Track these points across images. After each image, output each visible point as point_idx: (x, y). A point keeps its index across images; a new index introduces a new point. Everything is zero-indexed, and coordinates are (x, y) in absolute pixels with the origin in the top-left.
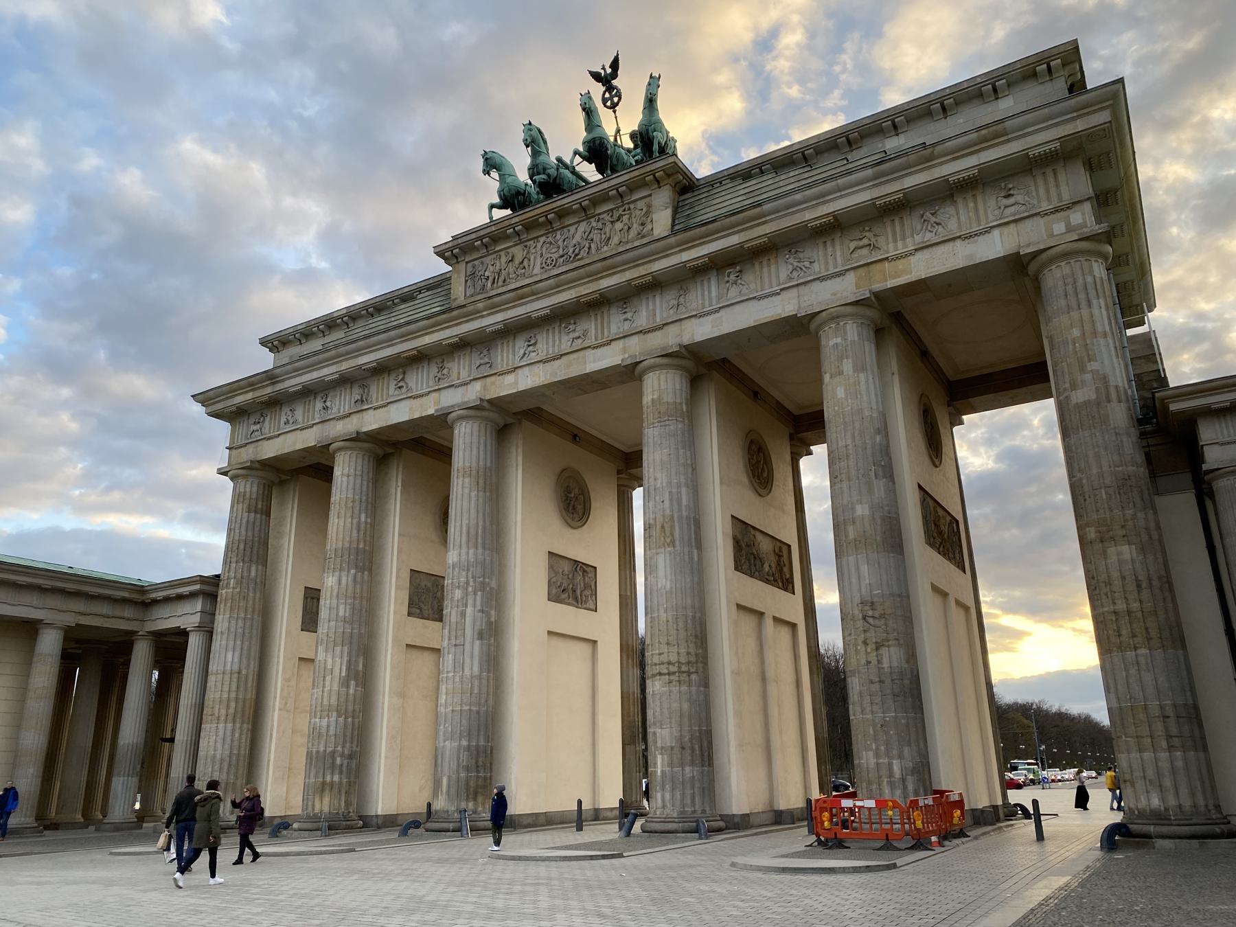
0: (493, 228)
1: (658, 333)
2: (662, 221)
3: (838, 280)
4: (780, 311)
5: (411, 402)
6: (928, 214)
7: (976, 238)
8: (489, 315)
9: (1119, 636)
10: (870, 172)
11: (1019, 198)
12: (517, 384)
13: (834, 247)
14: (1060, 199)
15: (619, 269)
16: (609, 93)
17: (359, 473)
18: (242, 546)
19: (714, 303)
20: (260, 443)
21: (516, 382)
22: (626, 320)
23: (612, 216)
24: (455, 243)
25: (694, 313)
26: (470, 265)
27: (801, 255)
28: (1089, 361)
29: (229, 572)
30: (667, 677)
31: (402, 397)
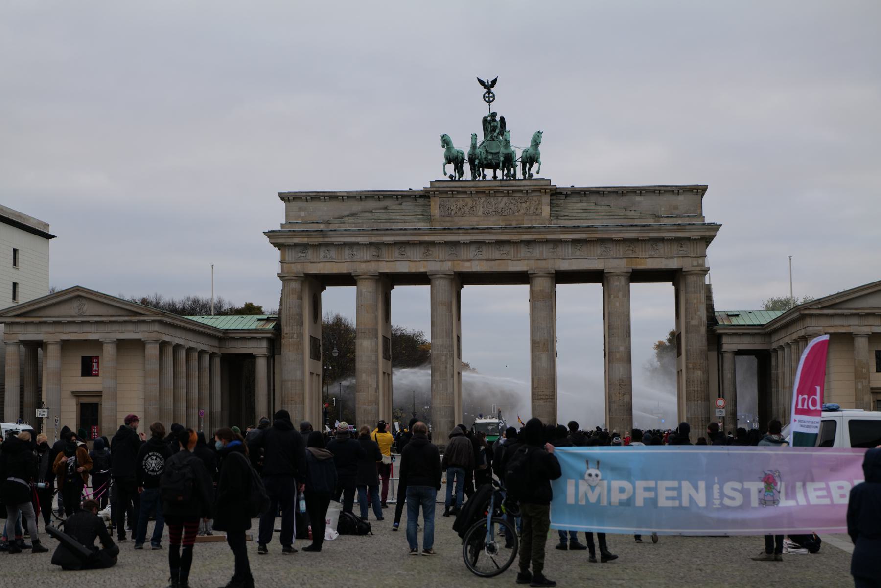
0: (460, 189)
1: (544, 261)
2: (546, 210)
4: (596, 266)
6: (654, 245)
9: (694, 397)
10: (639, 228)
13: (619, 246)
14: (697, 254)
16: (489, 95)
17: (374, 291)
18: (297, 317)
19: (570, 255)
20: (305, 264)
22: (528, 251)
24: (437, 189)
26: (441, 199)
28: (699, 311)
29: (292, 330)
30: (545, 400)
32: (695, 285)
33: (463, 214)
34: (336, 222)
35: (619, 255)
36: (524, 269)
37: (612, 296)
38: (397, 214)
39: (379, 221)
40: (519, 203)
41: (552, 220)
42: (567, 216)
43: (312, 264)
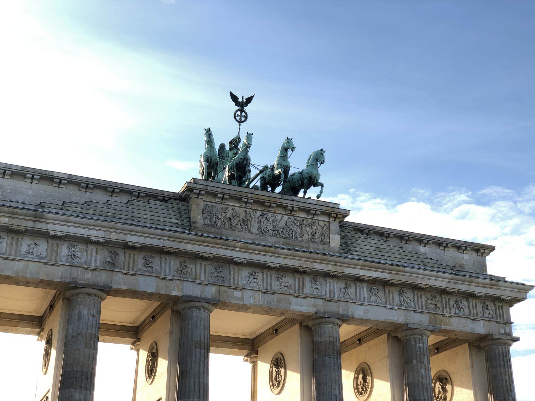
0: (235, 193)
1: (334, 304)
2: (335, 241)
3: (421, 314)
4: (396, 319)
5: (158, 278)
6: (460, 302)
7: (475, 321)
8: (239, 251)
10: (450, 276)
11: (491, 312)
12: (243, 299)
13: (421, 298)
15: (327, 262)
16: (241, 113)
19: (366, 300)
21: (242, 299)
22: (315, 288)
25: (355, 302)
27: (406, 295)
31: (152, 275)
32: (505, 358)
34: (53, 206)
35: (422, 309)
36: (311, 310)
37: (415, 362)
39: (119, 216)
43: (7, 261)
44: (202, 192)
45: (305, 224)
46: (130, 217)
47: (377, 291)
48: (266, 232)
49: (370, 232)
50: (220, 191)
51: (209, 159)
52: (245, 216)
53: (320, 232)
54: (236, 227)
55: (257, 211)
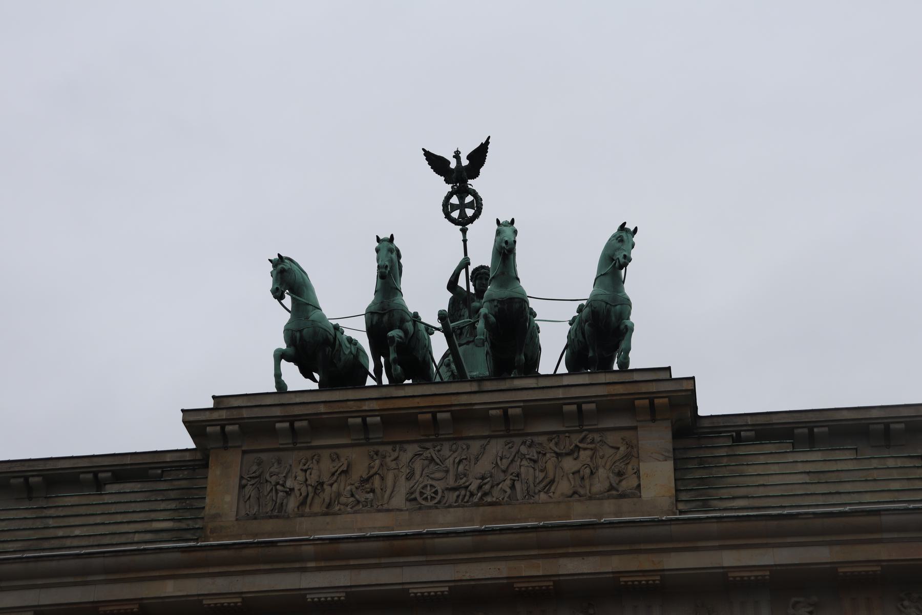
0: (322, 409)
8: (319, 569)
15: (600, 549)
16: (461, 199)
23: (556, 444)
24: (235, 414)
33: (329, 505)
38: (78, 521)
40: (548, 455)
41: (681, 512)
42: (746, 497)
44: (229, 428)
45: (556, 450)
46: (31, 542)
47: (811, 609)
48: (429, 497)
49: (816, 430)
50: (278, 414)
51: (296, 337)
52: (370, 468)
53: (608, 467)
54: (339, 503)
55: (406, 446)
